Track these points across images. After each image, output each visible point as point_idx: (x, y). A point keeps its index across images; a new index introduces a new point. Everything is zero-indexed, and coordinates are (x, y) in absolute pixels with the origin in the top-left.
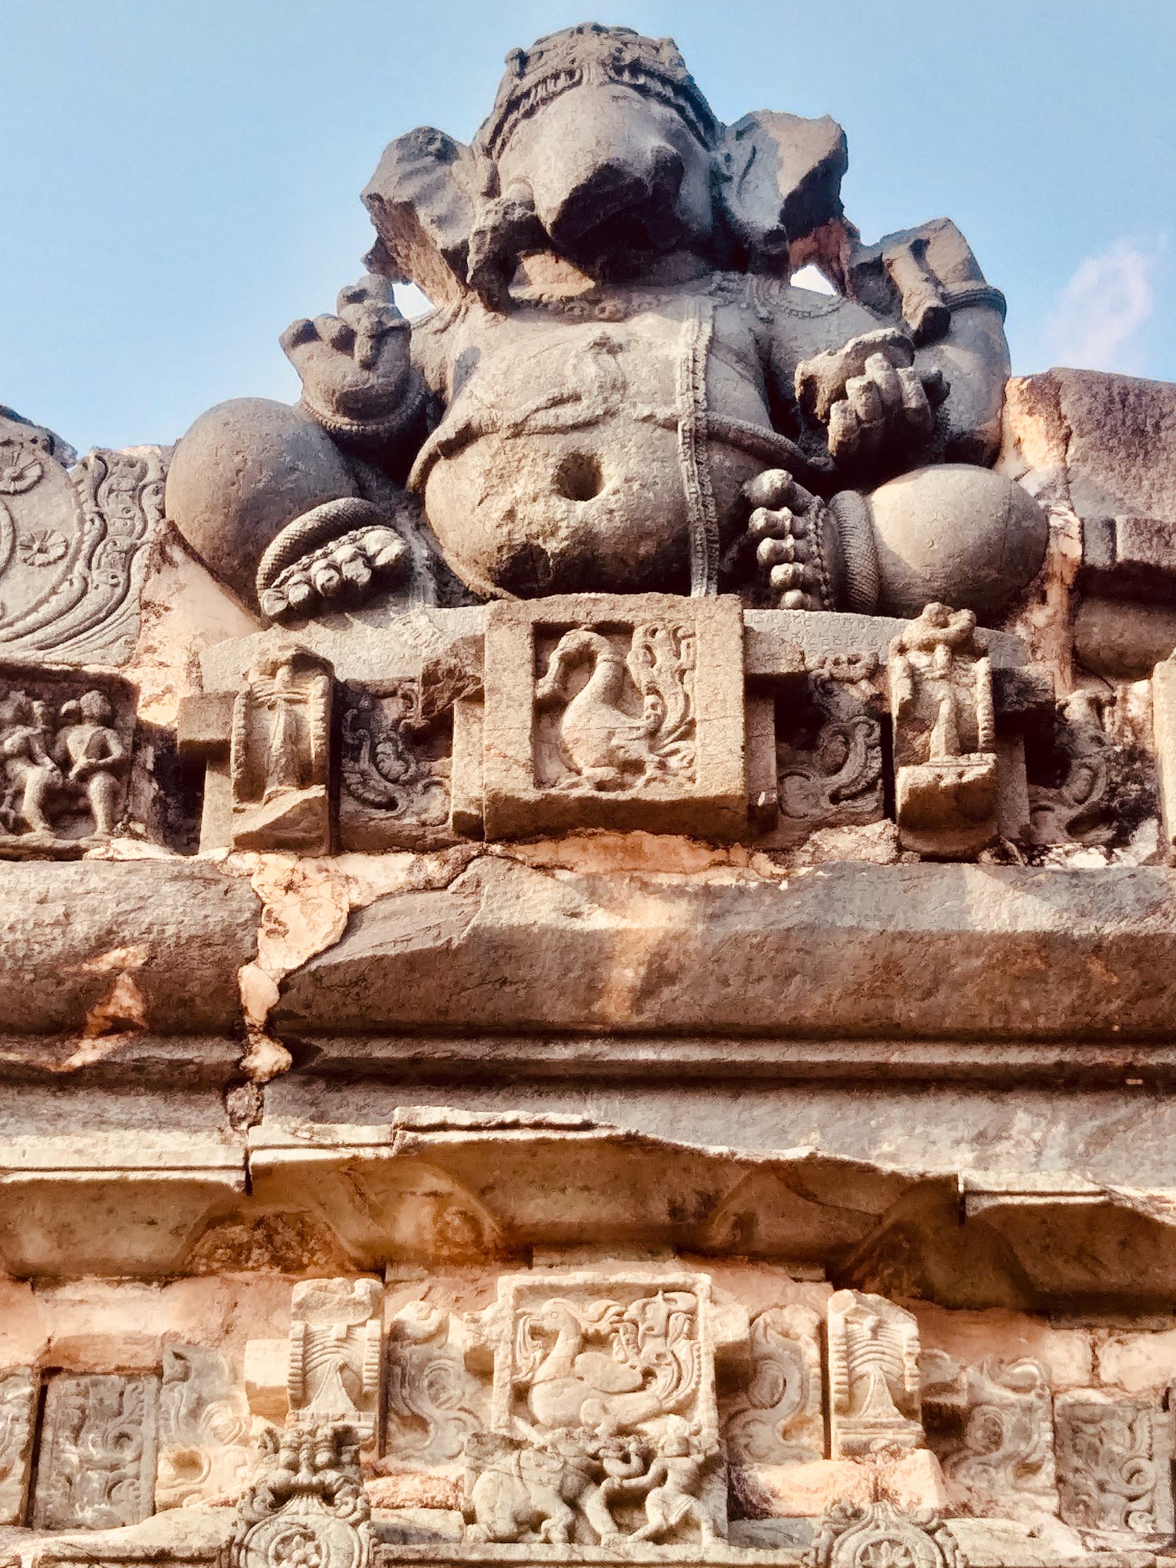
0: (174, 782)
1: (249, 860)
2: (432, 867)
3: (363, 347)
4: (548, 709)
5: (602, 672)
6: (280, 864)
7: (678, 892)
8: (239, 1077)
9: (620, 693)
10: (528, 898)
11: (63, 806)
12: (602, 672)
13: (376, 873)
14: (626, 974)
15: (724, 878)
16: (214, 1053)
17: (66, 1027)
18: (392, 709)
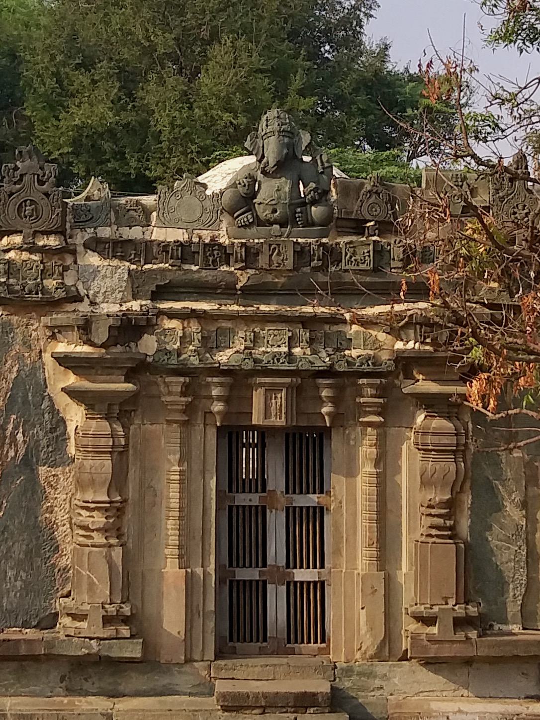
0: (225, 255)
1: (236, 271)
2: (257, 272)
3: (247, 187)
4: (271, 256)
5: (277, 251)
6: (240, 272)
7: (285, 277)
8: (236, 294)
9: (279, 254)
10: (269, 278)
11: (214, 261)
12: (277, 251)
13: (251, 272)
14: (280, 286)
15: (291, 275)
16: (234, 292)
17: (216, 289)
18: (252, 250)
